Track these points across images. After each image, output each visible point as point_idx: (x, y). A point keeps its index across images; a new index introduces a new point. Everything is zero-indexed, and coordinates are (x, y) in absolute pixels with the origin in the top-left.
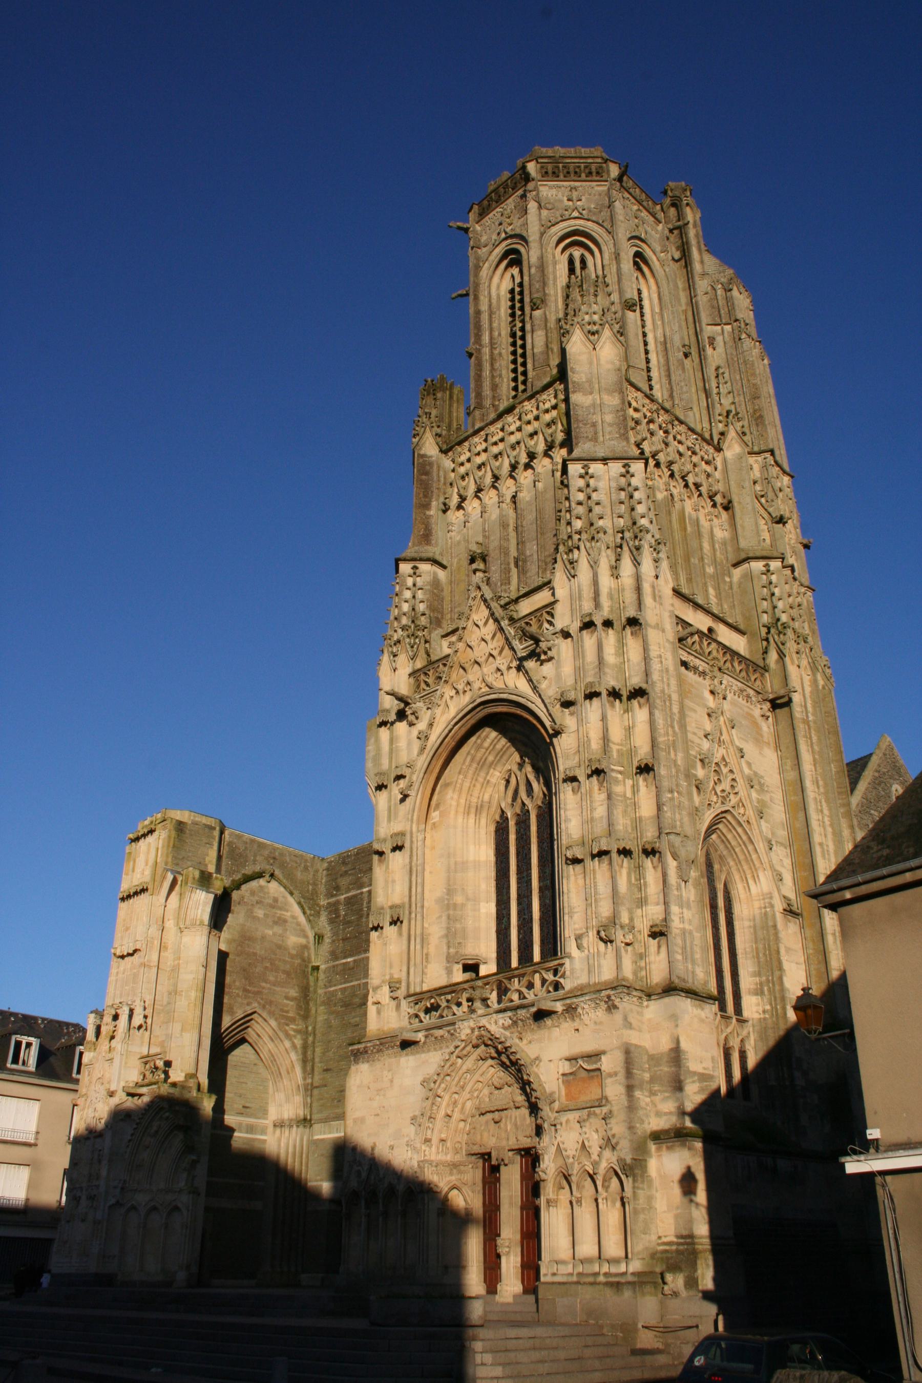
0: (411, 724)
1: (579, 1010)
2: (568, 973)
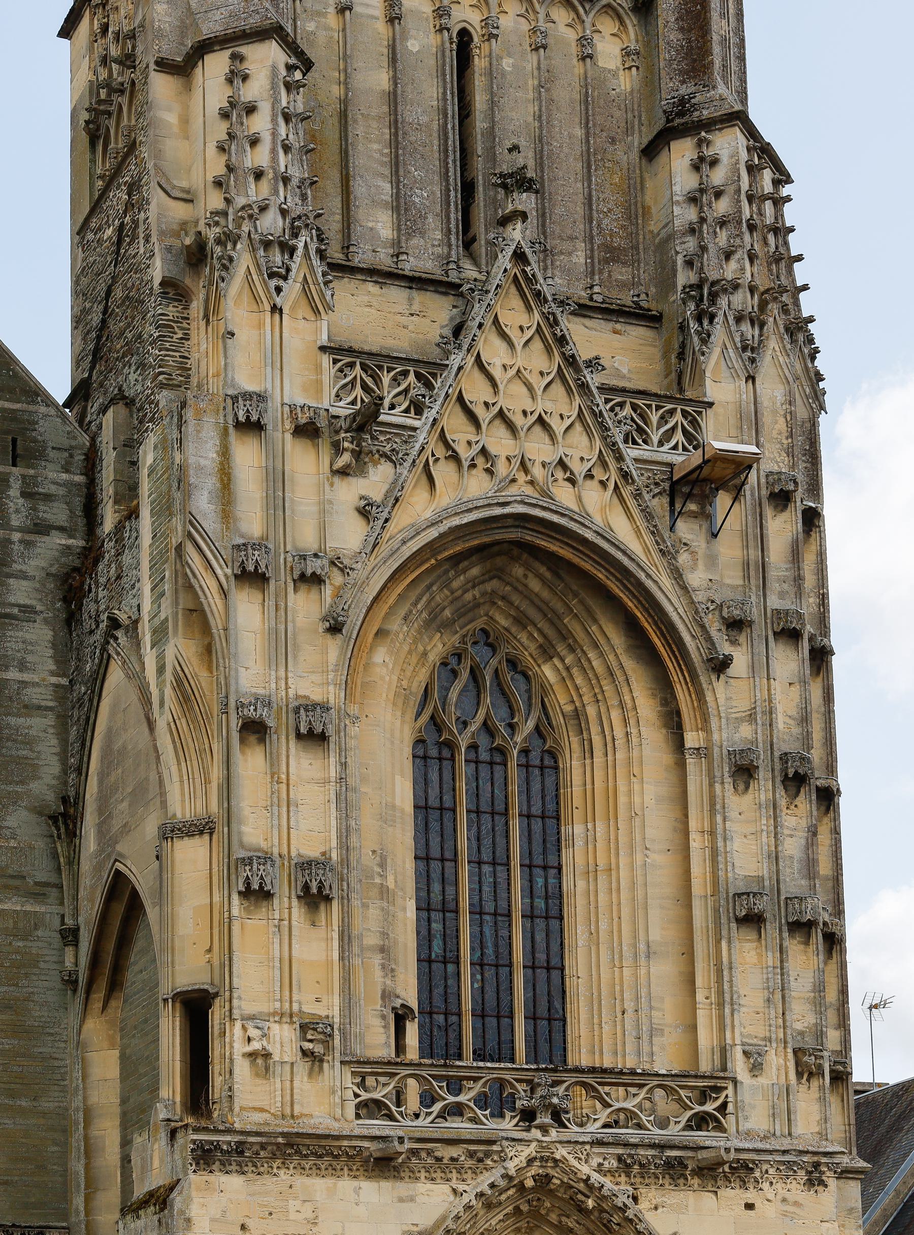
0: (343, 472)
1: (757, 1174)
2: (730, 1108)
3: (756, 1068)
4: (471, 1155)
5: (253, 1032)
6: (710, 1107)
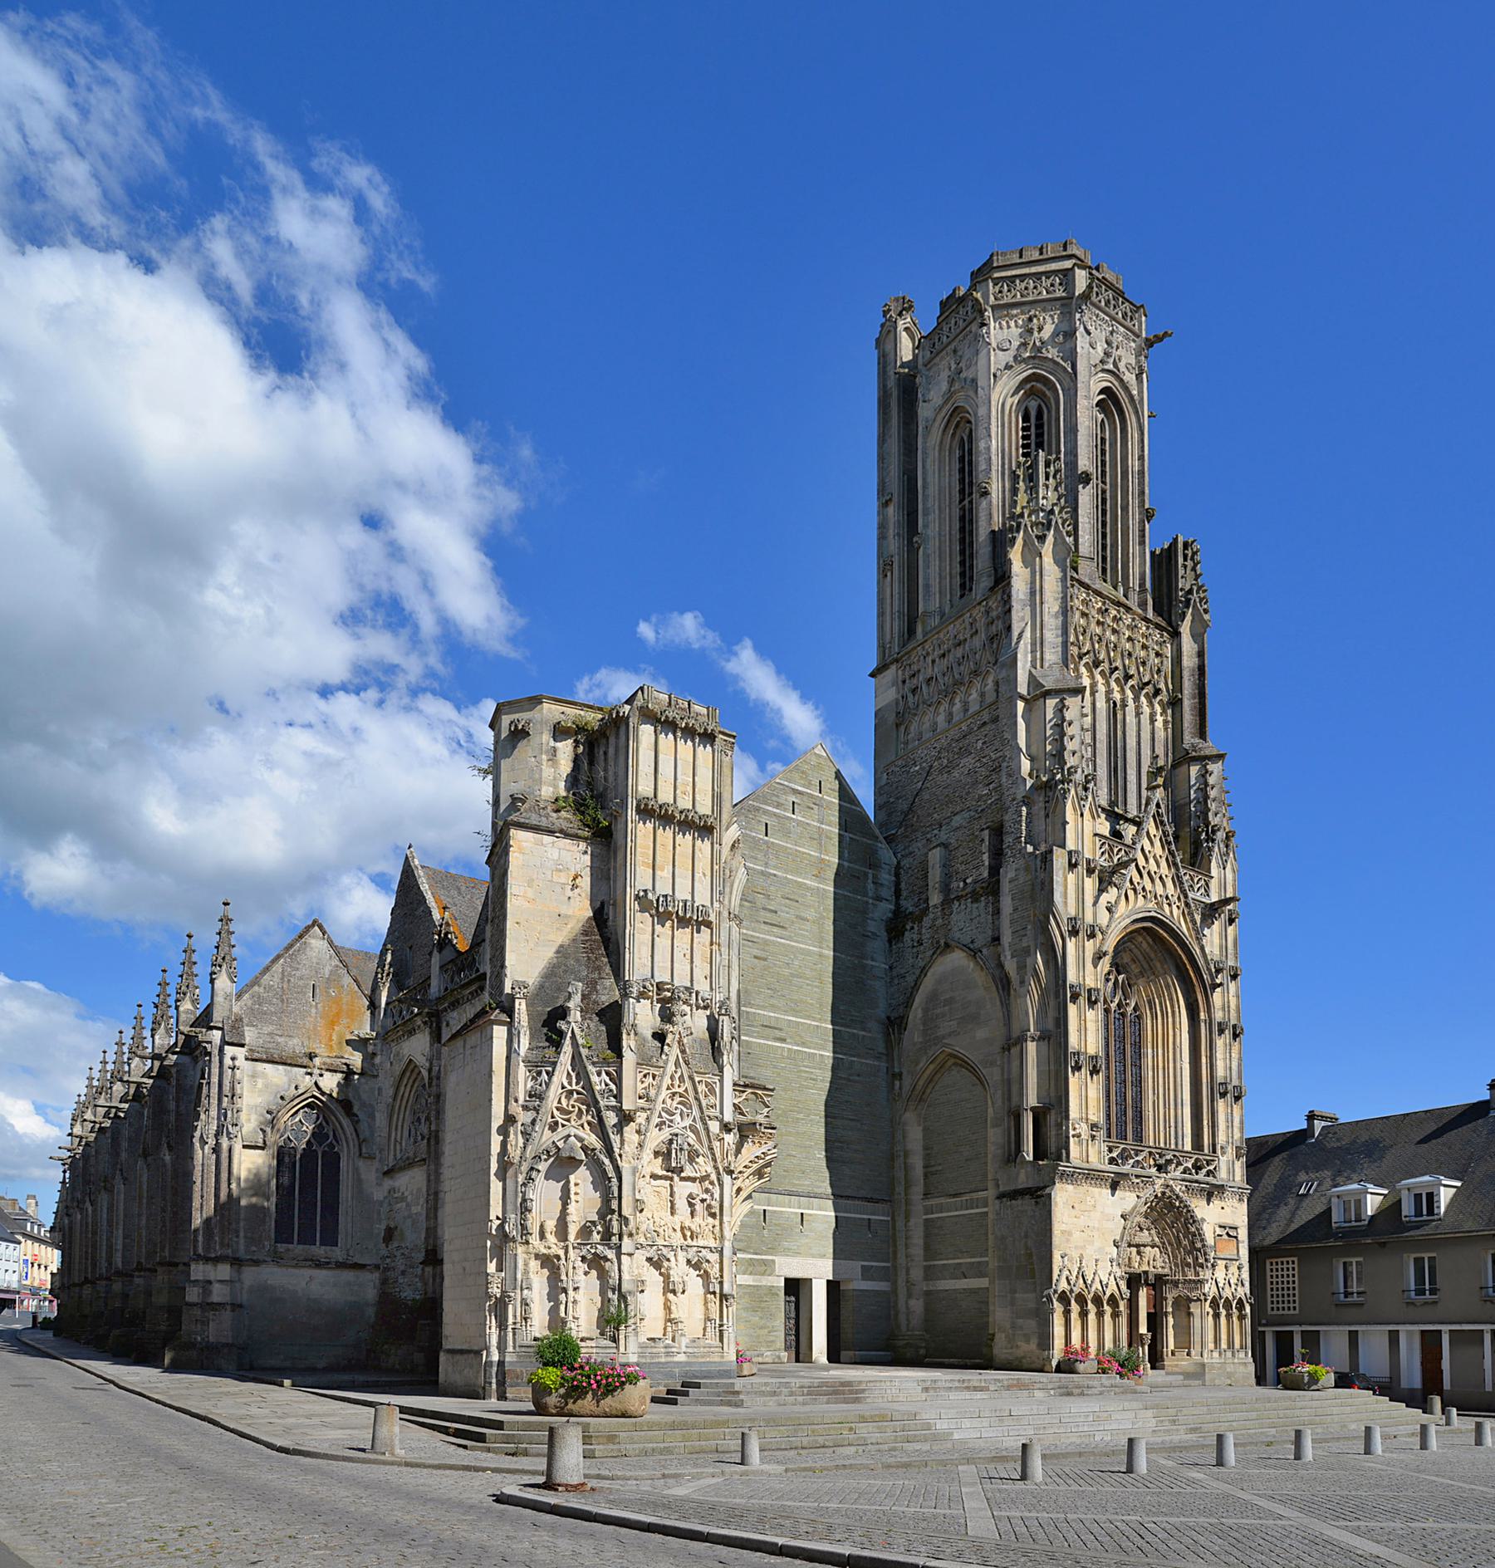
3: (1223, 1153)
4: (1142, 1181)
5: (1077, 1126)
6: (1211, 1168)
